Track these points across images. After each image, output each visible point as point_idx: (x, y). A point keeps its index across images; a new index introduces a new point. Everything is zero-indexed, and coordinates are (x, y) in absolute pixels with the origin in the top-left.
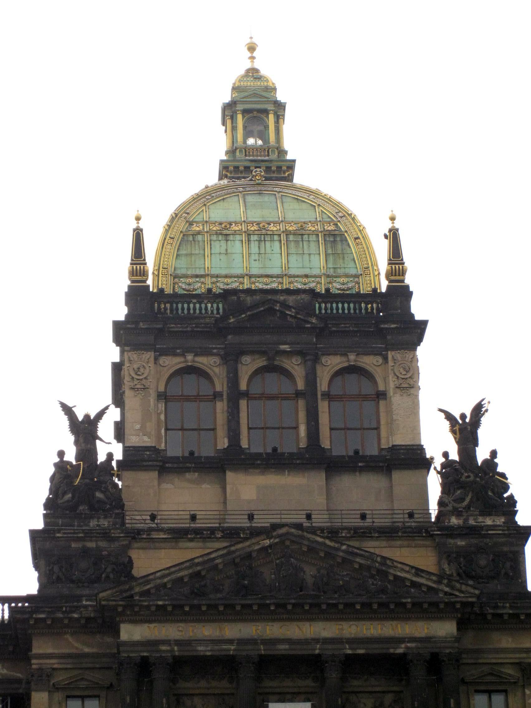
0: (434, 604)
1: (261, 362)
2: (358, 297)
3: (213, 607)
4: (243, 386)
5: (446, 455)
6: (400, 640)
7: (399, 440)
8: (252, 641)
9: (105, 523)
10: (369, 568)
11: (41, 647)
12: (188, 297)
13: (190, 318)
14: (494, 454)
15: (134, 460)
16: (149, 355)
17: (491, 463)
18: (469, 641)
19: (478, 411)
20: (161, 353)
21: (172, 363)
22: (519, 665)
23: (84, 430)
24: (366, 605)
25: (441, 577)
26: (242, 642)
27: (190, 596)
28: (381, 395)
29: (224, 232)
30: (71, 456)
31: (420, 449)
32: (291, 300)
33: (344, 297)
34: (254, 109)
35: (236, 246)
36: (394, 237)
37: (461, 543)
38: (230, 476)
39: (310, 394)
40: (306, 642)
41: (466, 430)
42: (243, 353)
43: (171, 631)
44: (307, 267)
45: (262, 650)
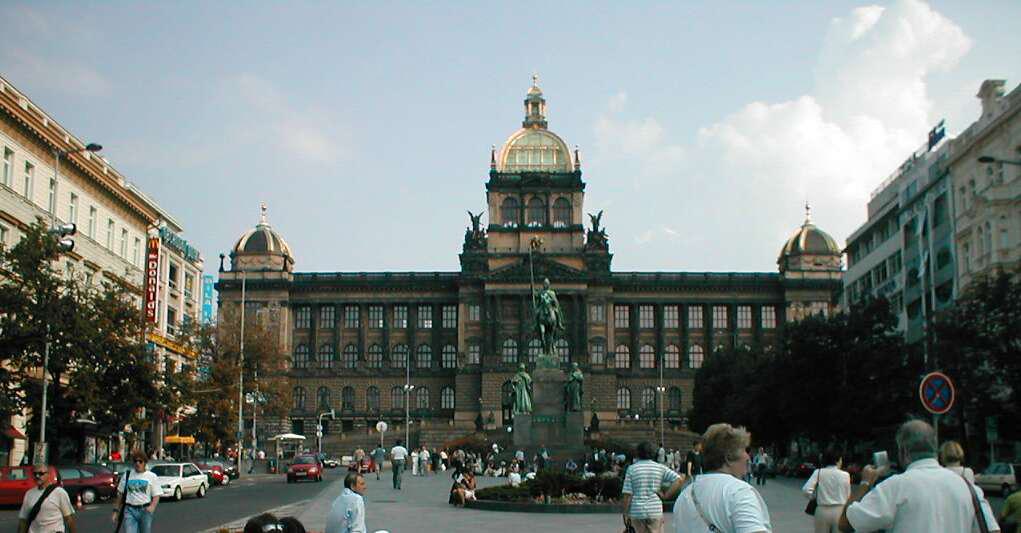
2: (566, 174)
4: (527, 203)
6: (568, 291)
7: (576, 222)
9: (481, 251)
11: (462, 290)
15: (491, 229)
16: (496, 194)
17: (603, 232)
18: (592, 289)
19: (601, 212)
21: (503, 196)
23: (476, 221)
25: (583, 272)
26: (522, 291)
27: (506, 276)
28: (571, 208)
30: (471, 229)
31: (581, 226)
32: (542, 176)
33: (562, 174)
34: (535, 102)
35: (525, 155)
36: (576, 152)
38: (521, 235)
39: (547, 205)
41: (596, 221)
43: (500, 287)
44: (546, 163)
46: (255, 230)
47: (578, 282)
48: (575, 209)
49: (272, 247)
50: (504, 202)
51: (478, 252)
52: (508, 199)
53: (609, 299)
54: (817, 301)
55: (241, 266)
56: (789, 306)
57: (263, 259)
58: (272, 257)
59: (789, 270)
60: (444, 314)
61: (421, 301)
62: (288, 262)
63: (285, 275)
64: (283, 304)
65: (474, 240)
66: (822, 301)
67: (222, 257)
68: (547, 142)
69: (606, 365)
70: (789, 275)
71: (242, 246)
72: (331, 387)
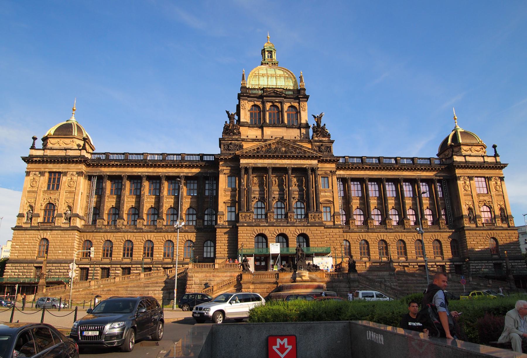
0: (313, 157)
1: (271, 104)
3: (262, 156)
4: (267, 109)
5: (314, 125)
6: (305, 164)
8: (271, 164)
9: (236, 137)
10: (298, 148)
12: (255, 89)
13: (255, 94)
14: (325, 125)
16: (246, 101)
18: (320, 165)
20: (249, 101)
21: (252, 103)
22: (331, 172)
24: (297, 156)
26: (268, 164)
29: (263, 75)
30: (228, 123)
32: (278, 90)
36: (301, 77)
37: (318, 143)
39: (282, 111)
40: (283, 164)
41: (318, 119)
42: (268, 102)
45: (273, 166)
46: (65, 122)
47: (312, 158)
48: (302, 113)
49: (75, 133)
50: (251, 109)
51: (234, 137)
52: (255, 105)
53: (333, 173)
54: (478, 177)
55: (49, 145)
56: (459, 180)
57: (67, 141)
58: (74, 140)
59: (455, 155)
60: (207, 187)
61: (190, 175)
62: (87, 146)
63: (84, 153)
64: (80, 174)
65: (231, 130)
66: (481, 177)
67: (35, 139)
68: (279, 72)
69: (334, 222)
70: (457, 159)
71: (52, 133)
72: (113, 240)
